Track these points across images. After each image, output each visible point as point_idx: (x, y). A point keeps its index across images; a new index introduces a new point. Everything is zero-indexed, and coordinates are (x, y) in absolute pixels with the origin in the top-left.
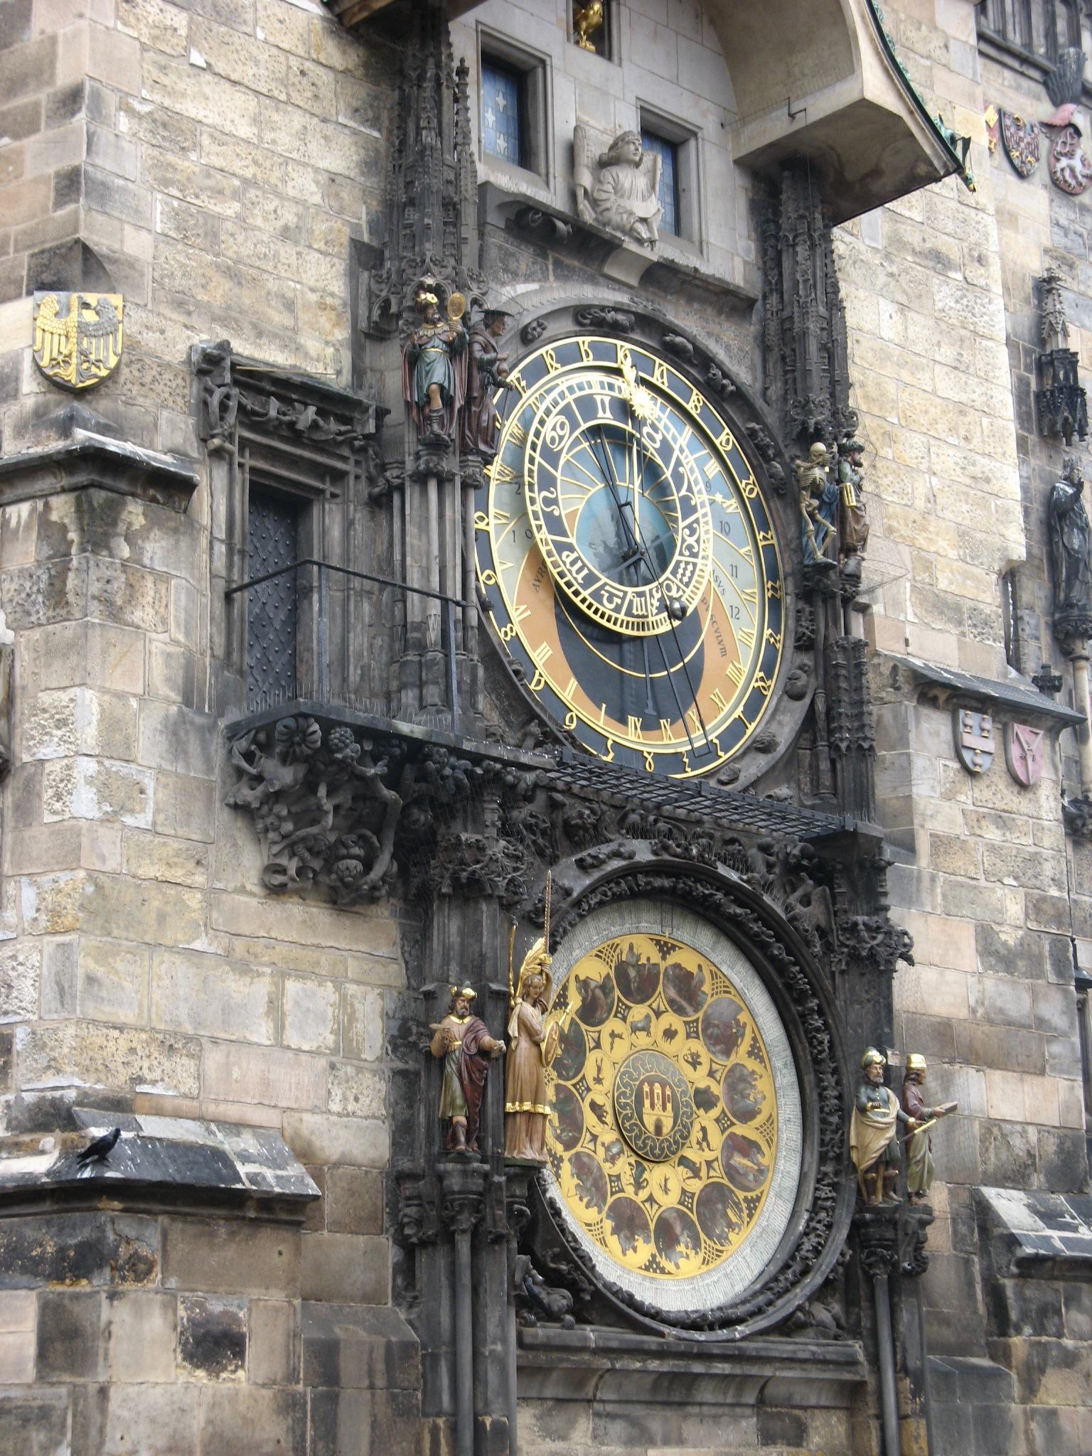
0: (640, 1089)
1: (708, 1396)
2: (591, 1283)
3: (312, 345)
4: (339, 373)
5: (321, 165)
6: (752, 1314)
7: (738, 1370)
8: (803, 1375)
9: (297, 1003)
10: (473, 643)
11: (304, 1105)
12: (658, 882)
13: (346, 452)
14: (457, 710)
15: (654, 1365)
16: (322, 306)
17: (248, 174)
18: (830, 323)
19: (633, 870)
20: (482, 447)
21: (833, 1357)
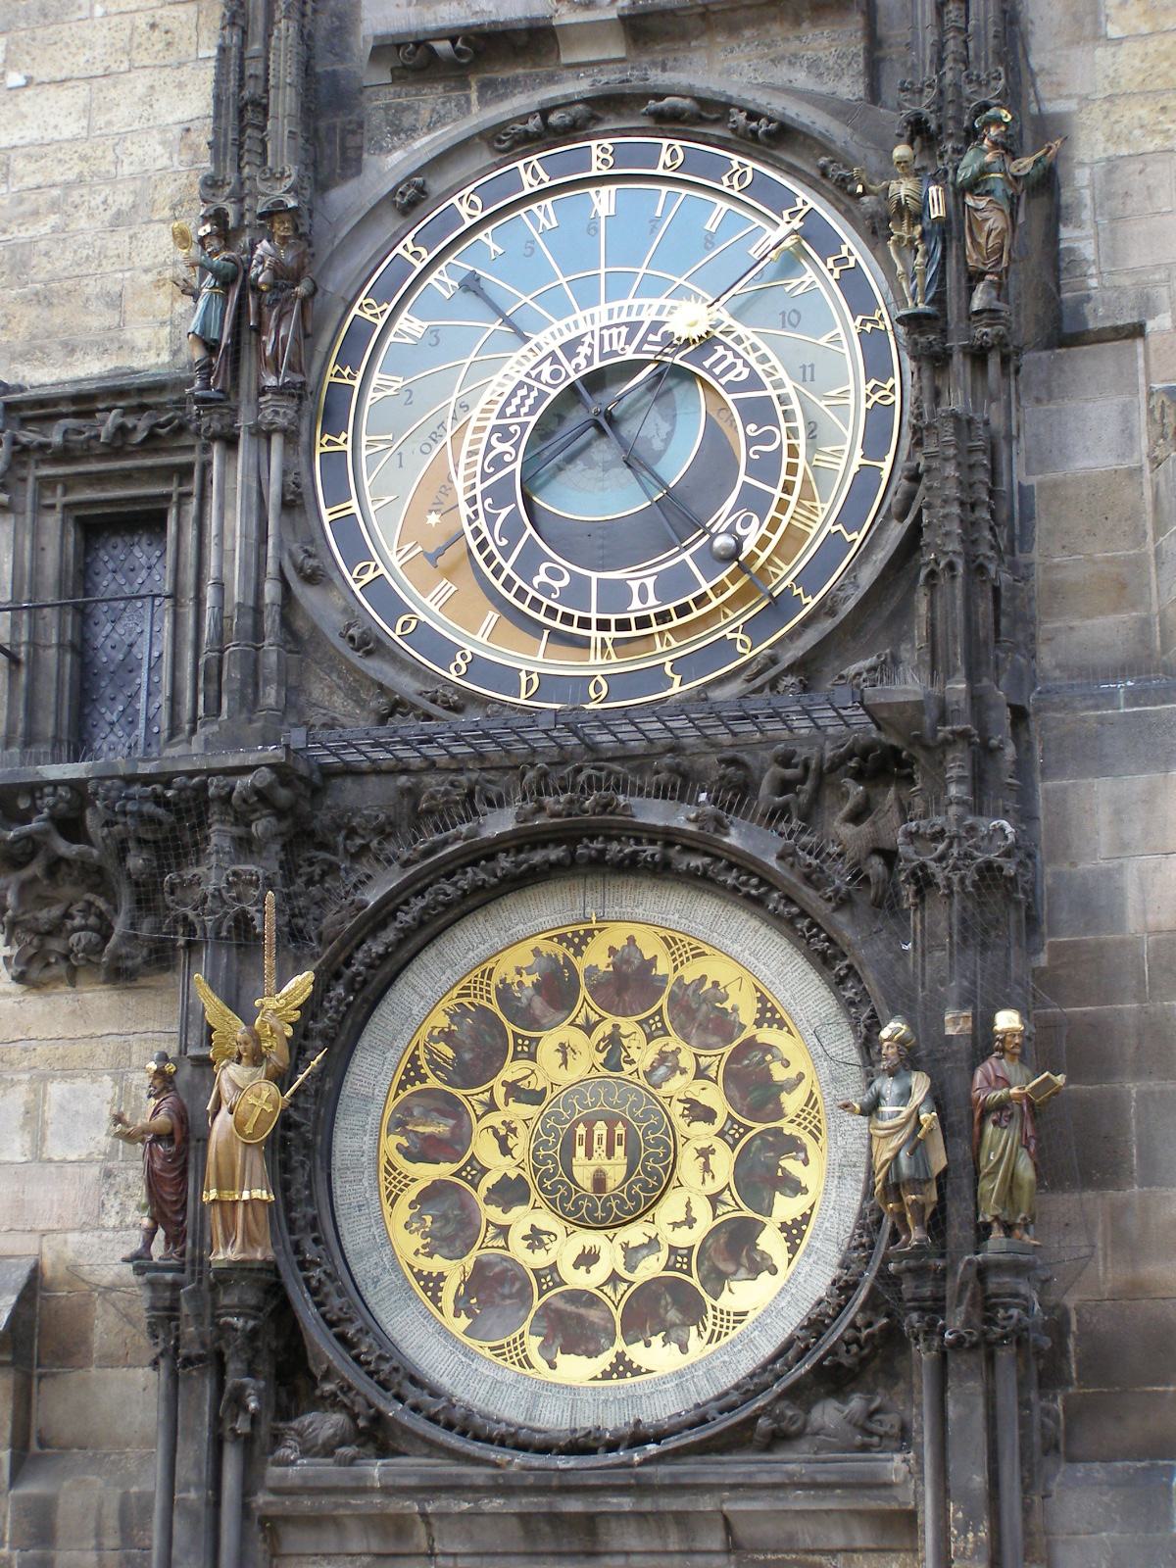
0: (570, 1137)
1: (633, 1543)
2: (370, 1406)
3: (140, 334)
4: (175, 353)
5: (170, 120)
6: (691, 1426)
7: (647, 1505)
8: (780, 1506)
9: (62, 1108)
10: (271, 622)
11: (69, 1224)
12: (537, 857)
13: (187, 440)
14: (224, 716)
15: (496, 1504)
16: (158, 284)
17: (71, 176)
19: (488, 852)
21: (833, 1478)
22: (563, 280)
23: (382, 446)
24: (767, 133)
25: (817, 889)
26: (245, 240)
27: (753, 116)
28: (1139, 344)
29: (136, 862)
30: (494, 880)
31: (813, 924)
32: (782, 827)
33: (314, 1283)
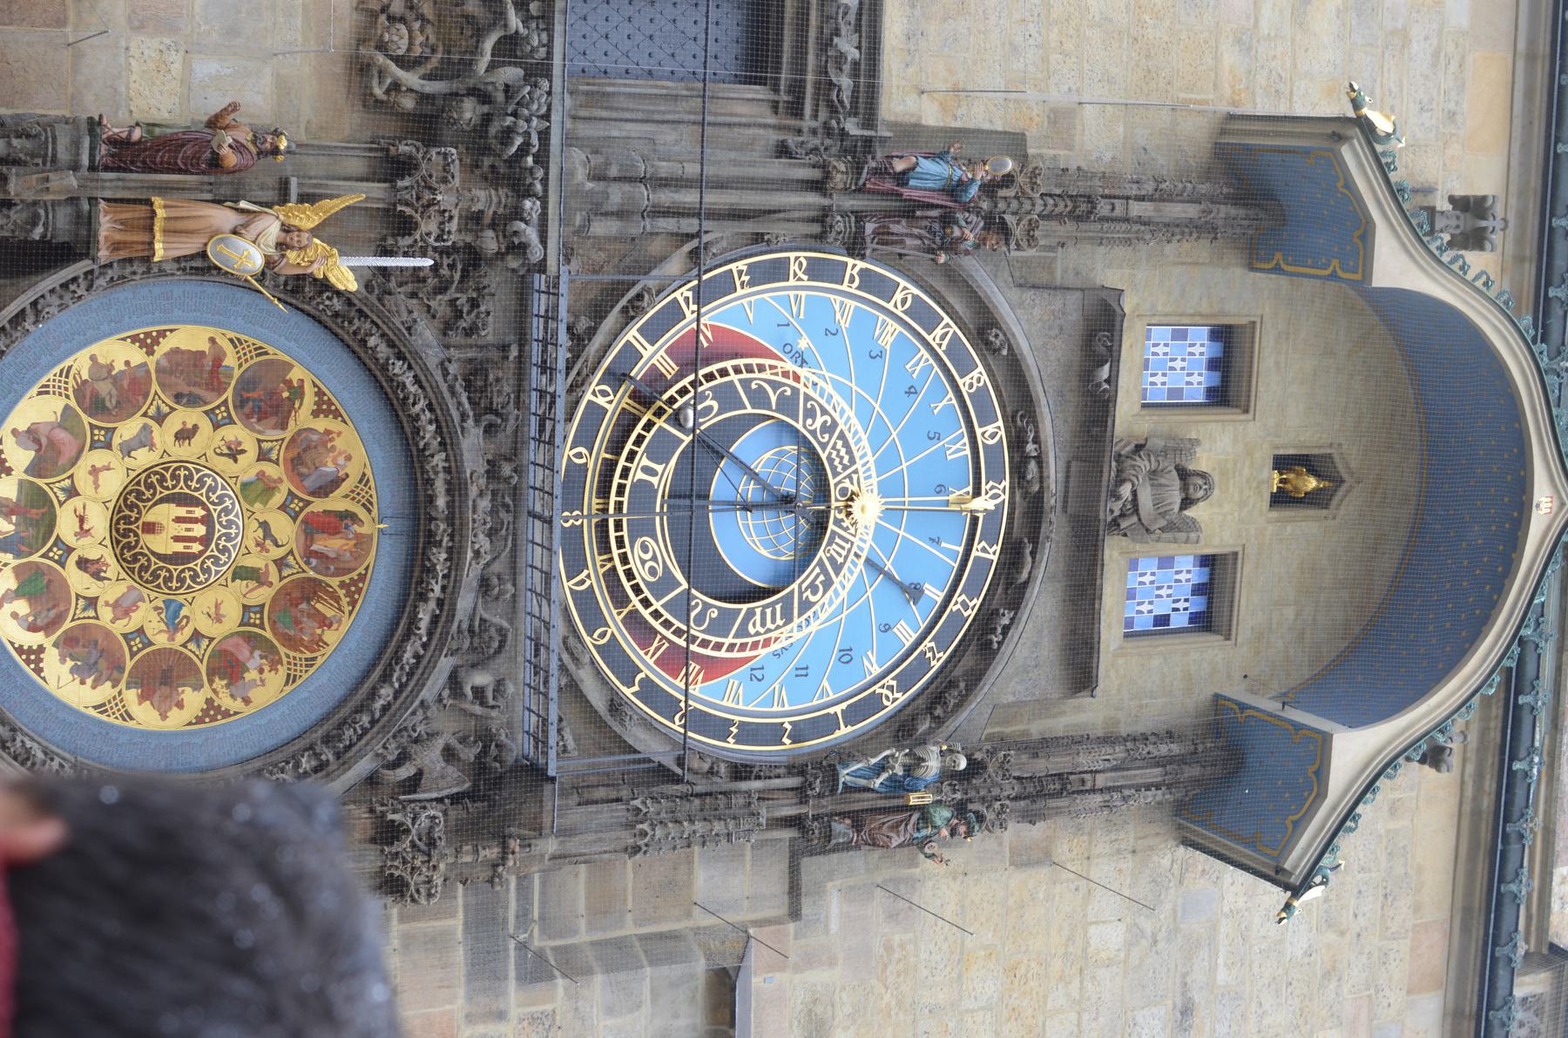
0: (197, 502)
12: (440, 486)
13: (823, 114)
18: (1093, 791)
19: (447, 442)
20: (870, 227)
22: (904, 466)
23: (795, 310)
24: (991, 642)
25: (394, 737)
26: (985, 205)
27: (1006, 629)
28: (784, 910)
29: (469, 111)
30: (421, 444)
31: (365, 731)
32: (446, 693)
33: (72, 287)
